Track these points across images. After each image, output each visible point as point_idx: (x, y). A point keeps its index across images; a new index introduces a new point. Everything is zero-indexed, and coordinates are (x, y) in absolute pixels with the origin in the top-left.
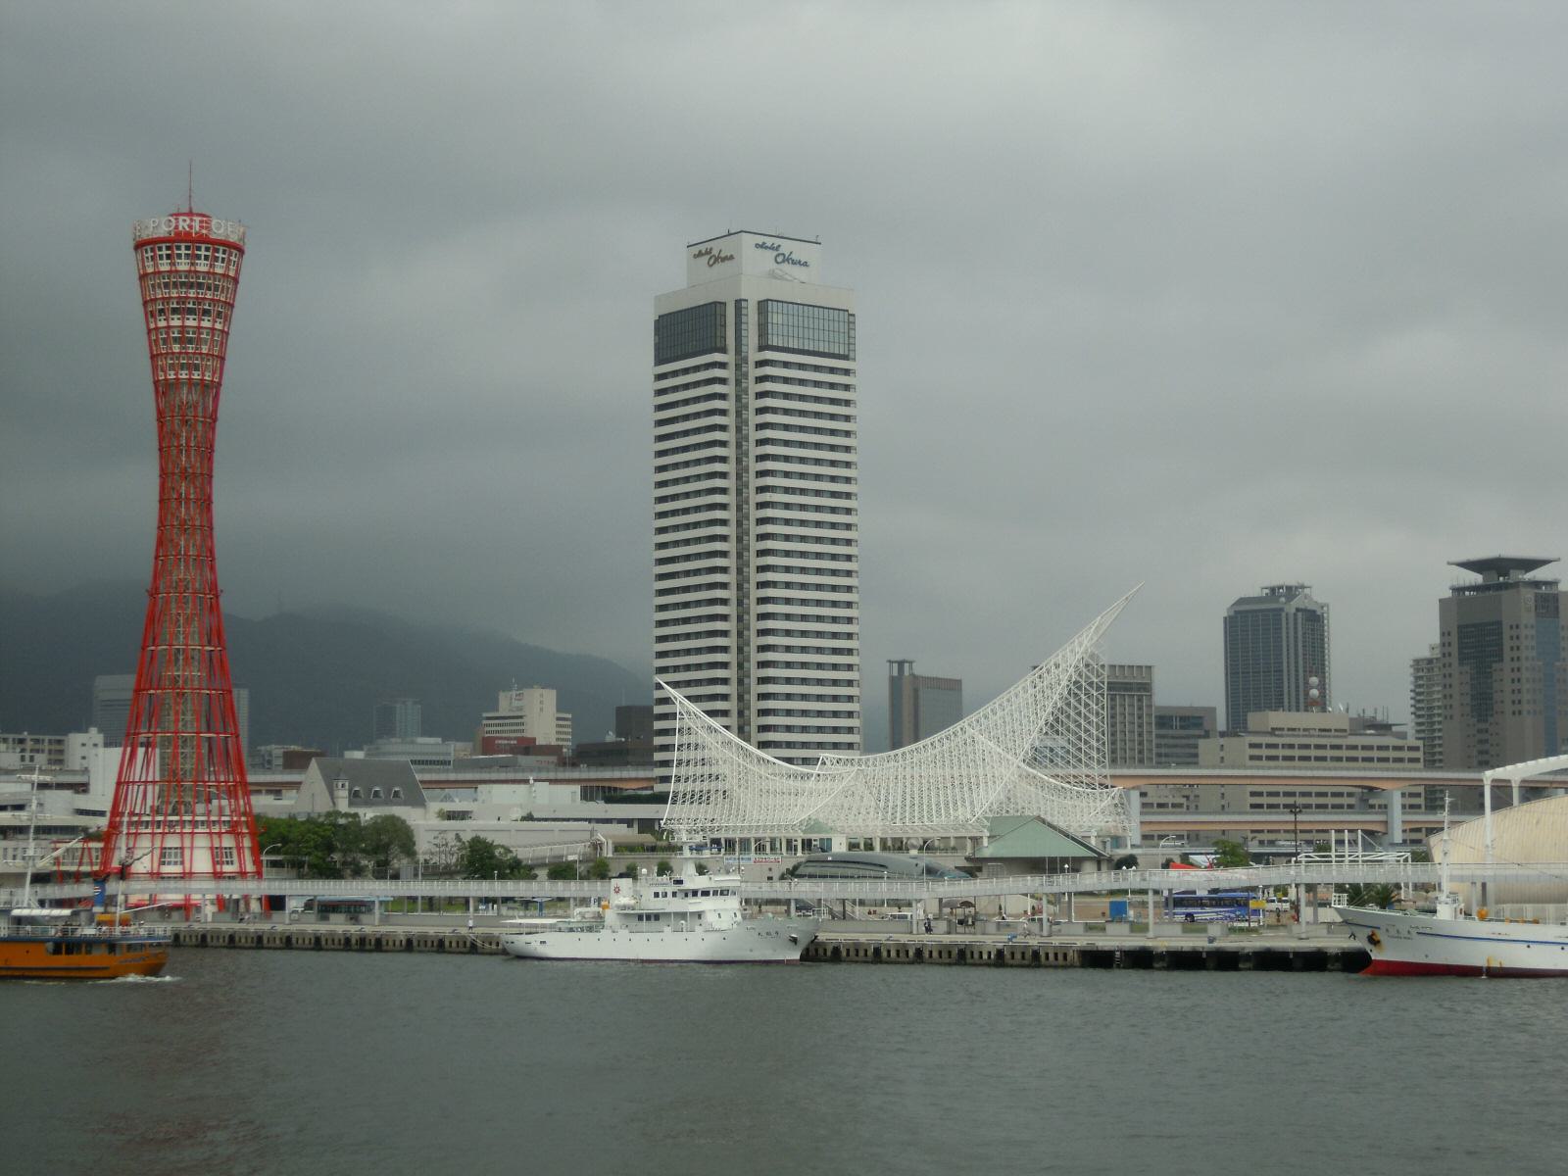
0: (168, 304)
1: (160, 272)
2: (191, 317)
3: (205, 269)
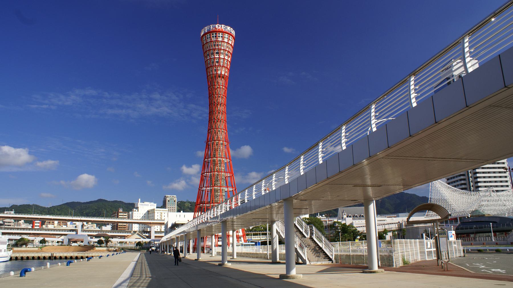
0: (215, 51)
1: (212, 41)
2: (222, 55)
3: (221, 40)
